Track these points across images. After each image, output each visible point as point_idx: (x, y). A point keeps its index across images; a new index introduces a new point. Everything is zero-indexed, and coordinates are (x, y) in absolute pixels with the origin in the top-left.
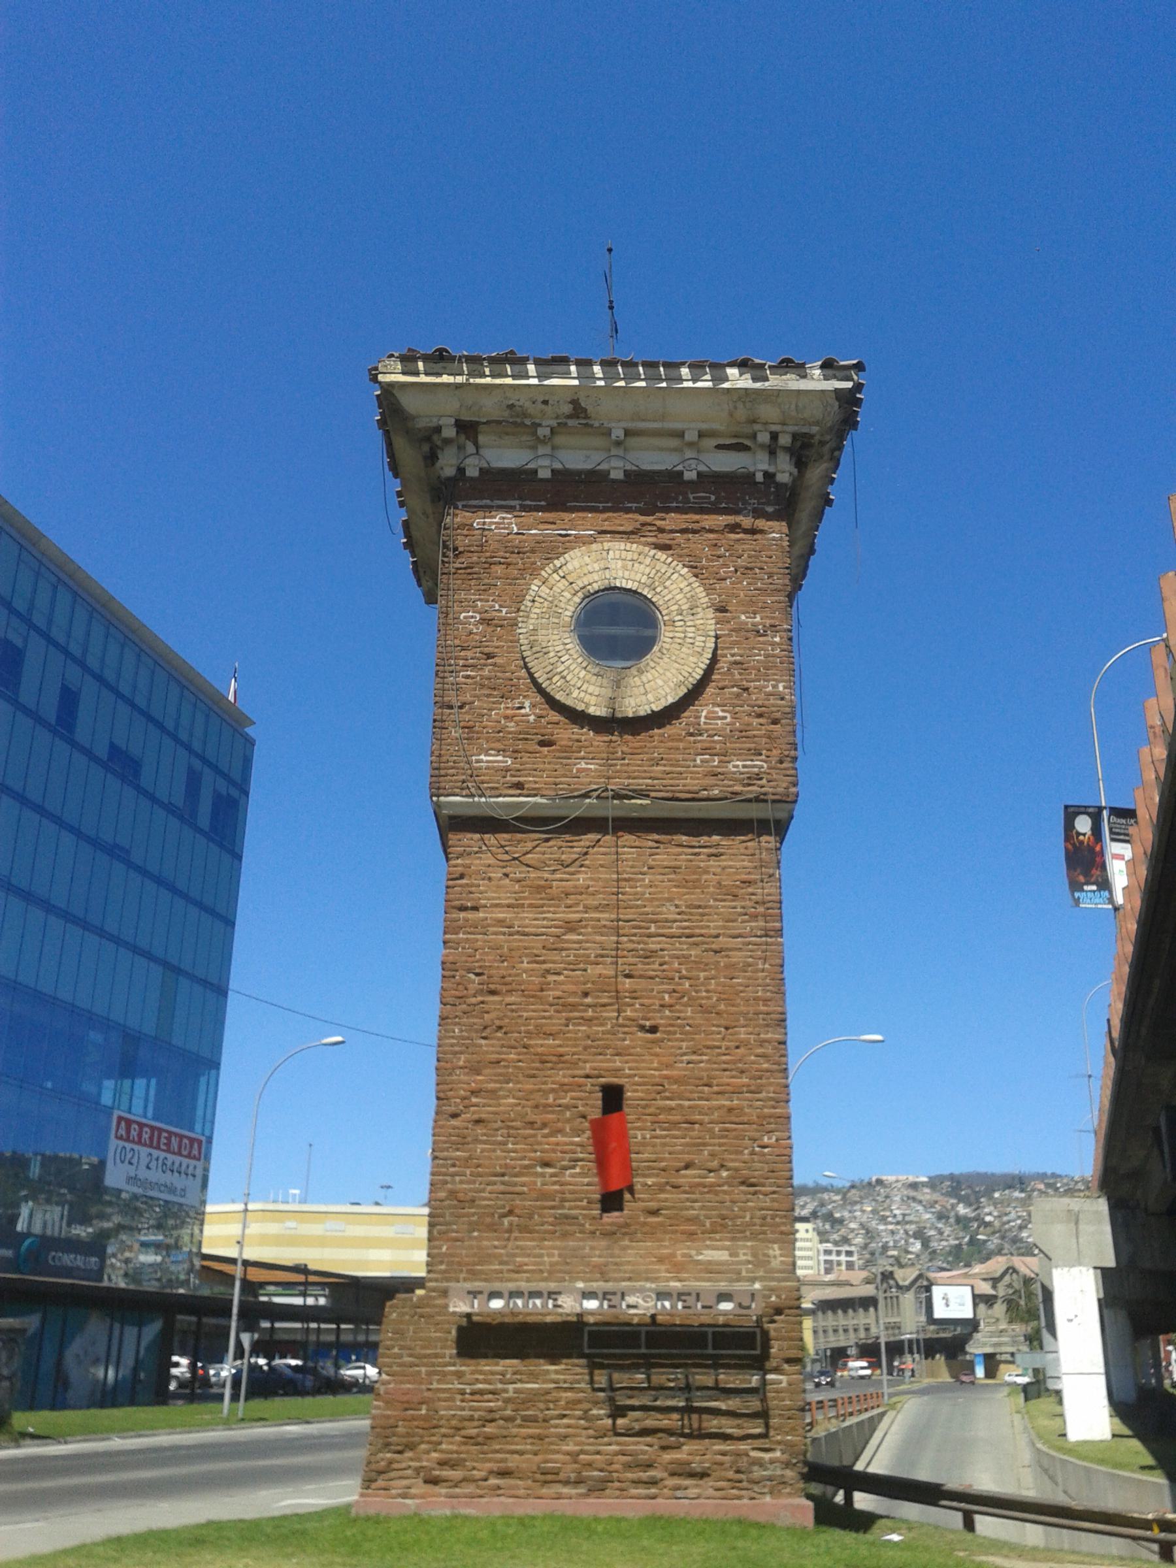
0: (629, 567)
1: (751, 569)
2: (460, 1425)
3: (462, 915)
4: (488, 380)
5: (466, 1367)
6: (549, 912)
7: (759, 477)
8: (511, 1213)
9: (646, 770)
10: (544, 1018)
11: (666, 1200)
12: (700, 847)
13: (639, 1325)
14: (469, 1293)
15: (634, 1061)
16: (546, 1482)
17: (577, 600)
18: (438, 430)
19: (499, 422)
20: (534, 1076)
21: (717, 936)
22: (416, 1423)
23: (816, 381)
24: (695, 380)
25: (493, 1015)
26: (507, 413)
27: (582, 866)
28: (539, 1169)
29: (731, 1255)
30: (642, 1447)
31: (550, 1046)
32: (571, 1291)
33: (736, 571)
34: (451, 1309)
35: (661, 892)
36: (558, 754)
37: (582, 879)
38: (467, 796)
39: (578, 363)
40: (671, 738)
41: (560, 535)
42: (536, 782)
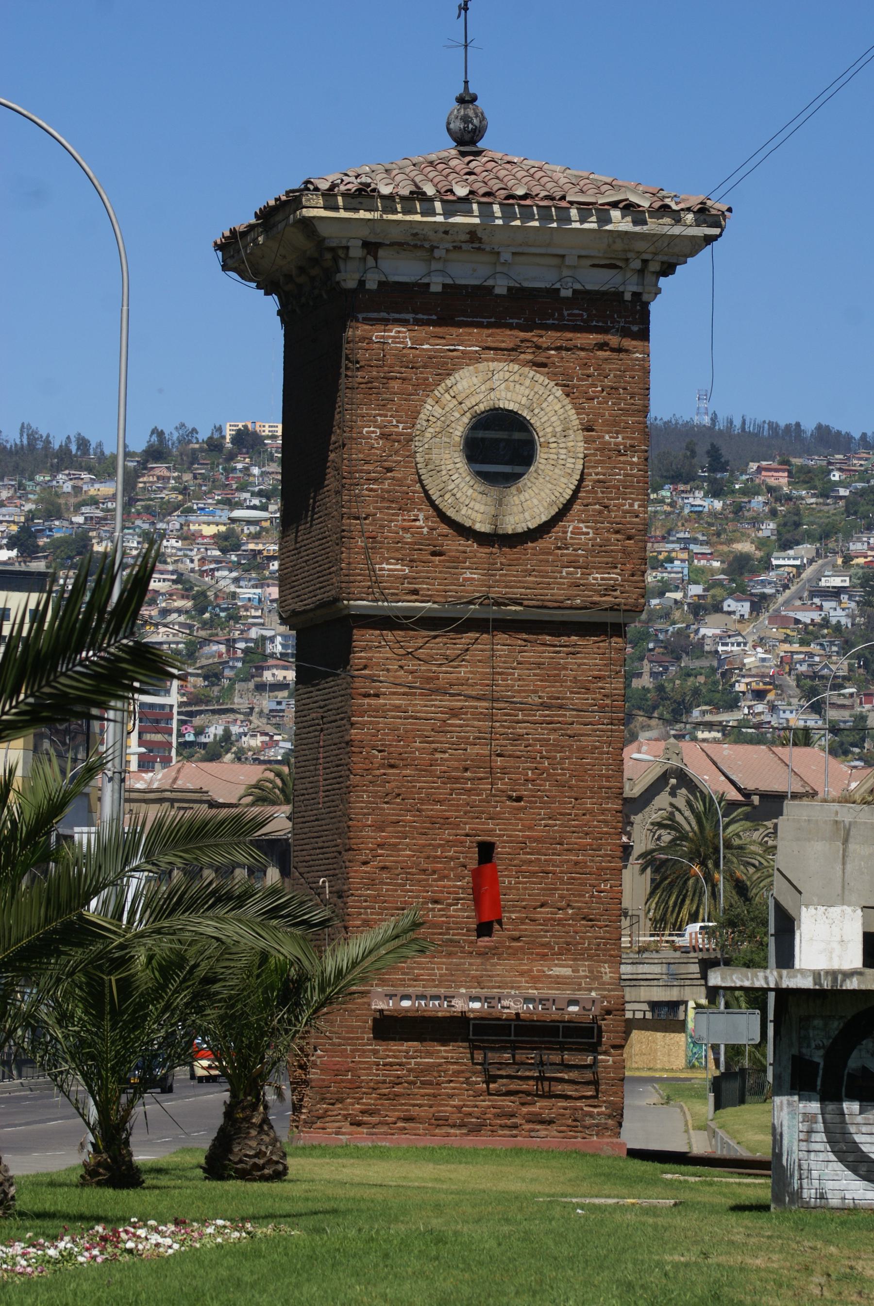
0: (511, 388)
1: (617, 389)
3: (366, 701)
7: (628, 297)
9: (522, 582)
10: (433, 788)
11: (526, 930)
12: (561, 646)
13: (506, 1020)
15: (504, 824)
17: (466, 420)
19: (400, 244)
24: (582, 221)
25: (394, 784)
27: (463, 660)
28: (430, 905)
30: (507, 1103)
31: (437, 810)
32: (461, 996)
33: (603, 390)
35: (527, 685)
42: (429, 590)
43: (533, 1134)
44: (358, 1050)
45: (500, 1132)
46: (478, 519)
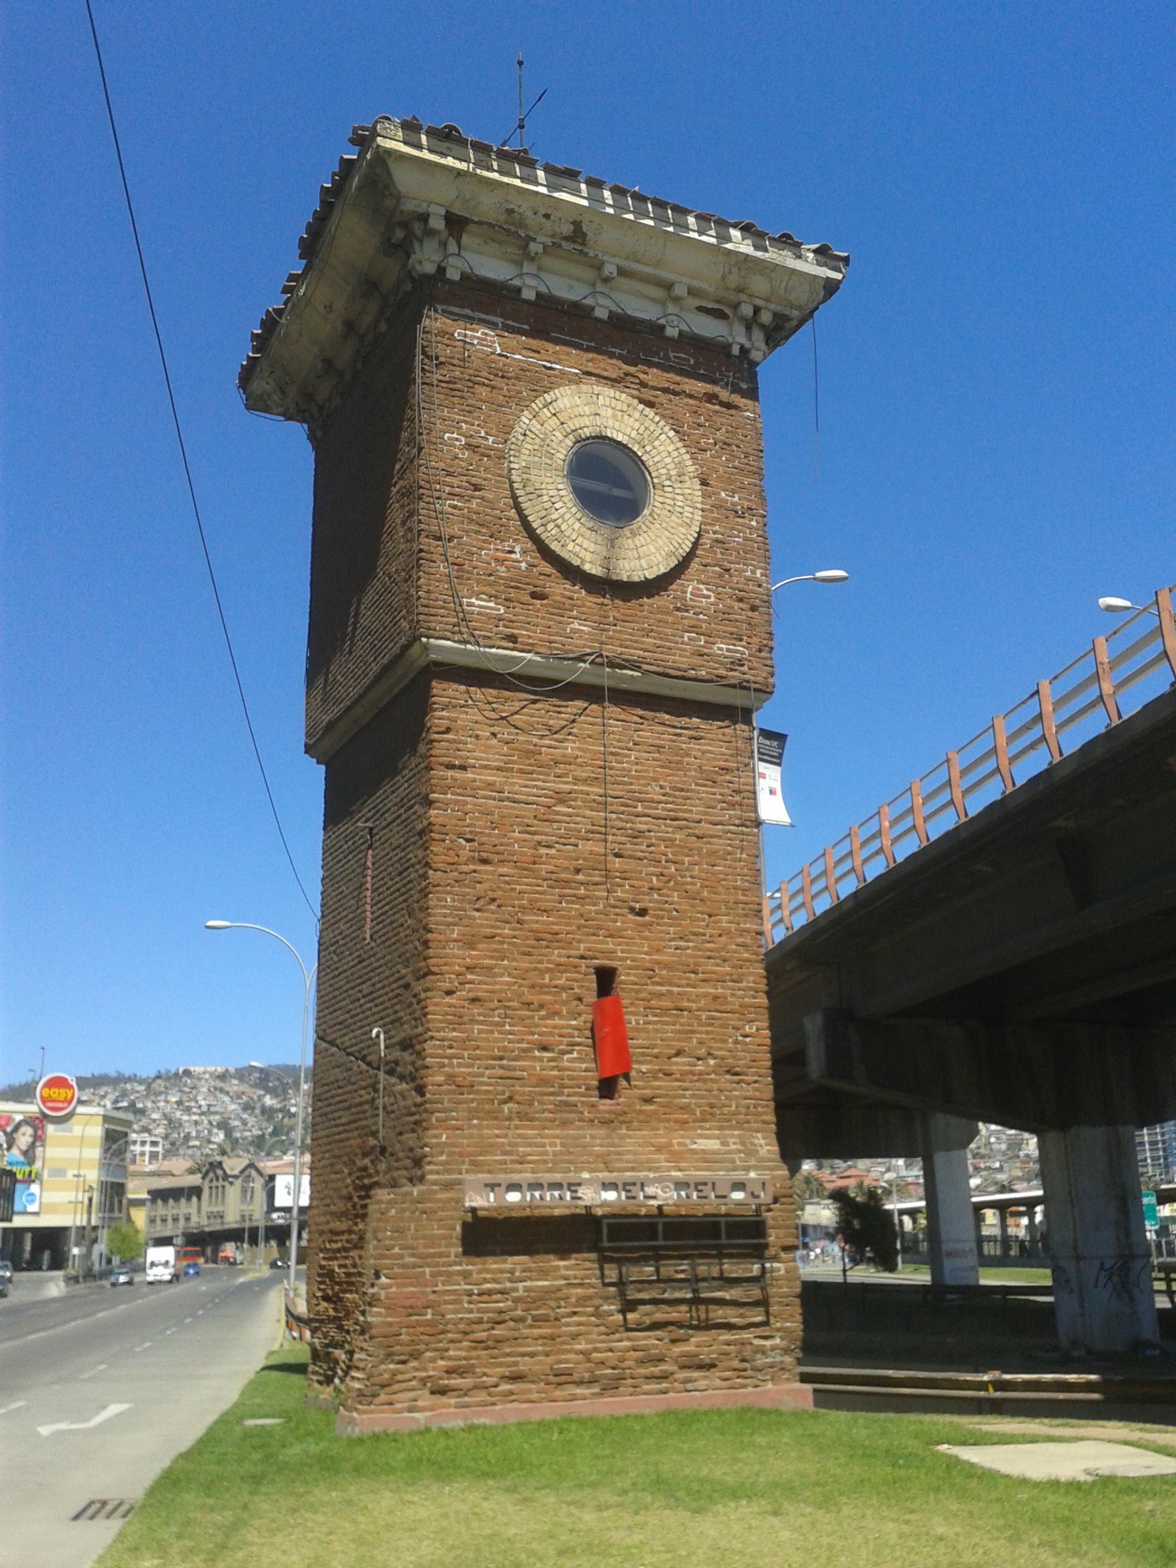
1: (729, 445)
2: (468, 1329)
3: (450, 773)
4: (495, 176)
5: (473, 1266)
6: (539, 780)
7: (736, 350)
8: (510, 1099)
10: (537, 892)
11: (660, 1088)
12: (682, 728)
14: (486, 1185)
15: (627, 944)
16: (560, 1384)
17: (569, 442)
18: (424, 218)
19: (492, 226)
20: (529, 954)
21: (699, 822)
22: (422, 1329)
23: (808, 265)
24: (701, 233)
25: (486, 886)
26: (503, 218)
27: (570, 734)
28: (537, 1053)
29: (722, 1144)
30: (650, 1340)
31: (543, 923)
32: (589, 1182)
34: (467, 1204)
35: (646, 771)
36: (551, 610)
37: (570, 748)
38: (459, 642)
39: (590, 182)
40: (660, 610)
41: (544, 366)
42: (530, 637)
43: (689, 1386)
44: (440, 1274)
45: (646, 1387)
46: (588, 559)
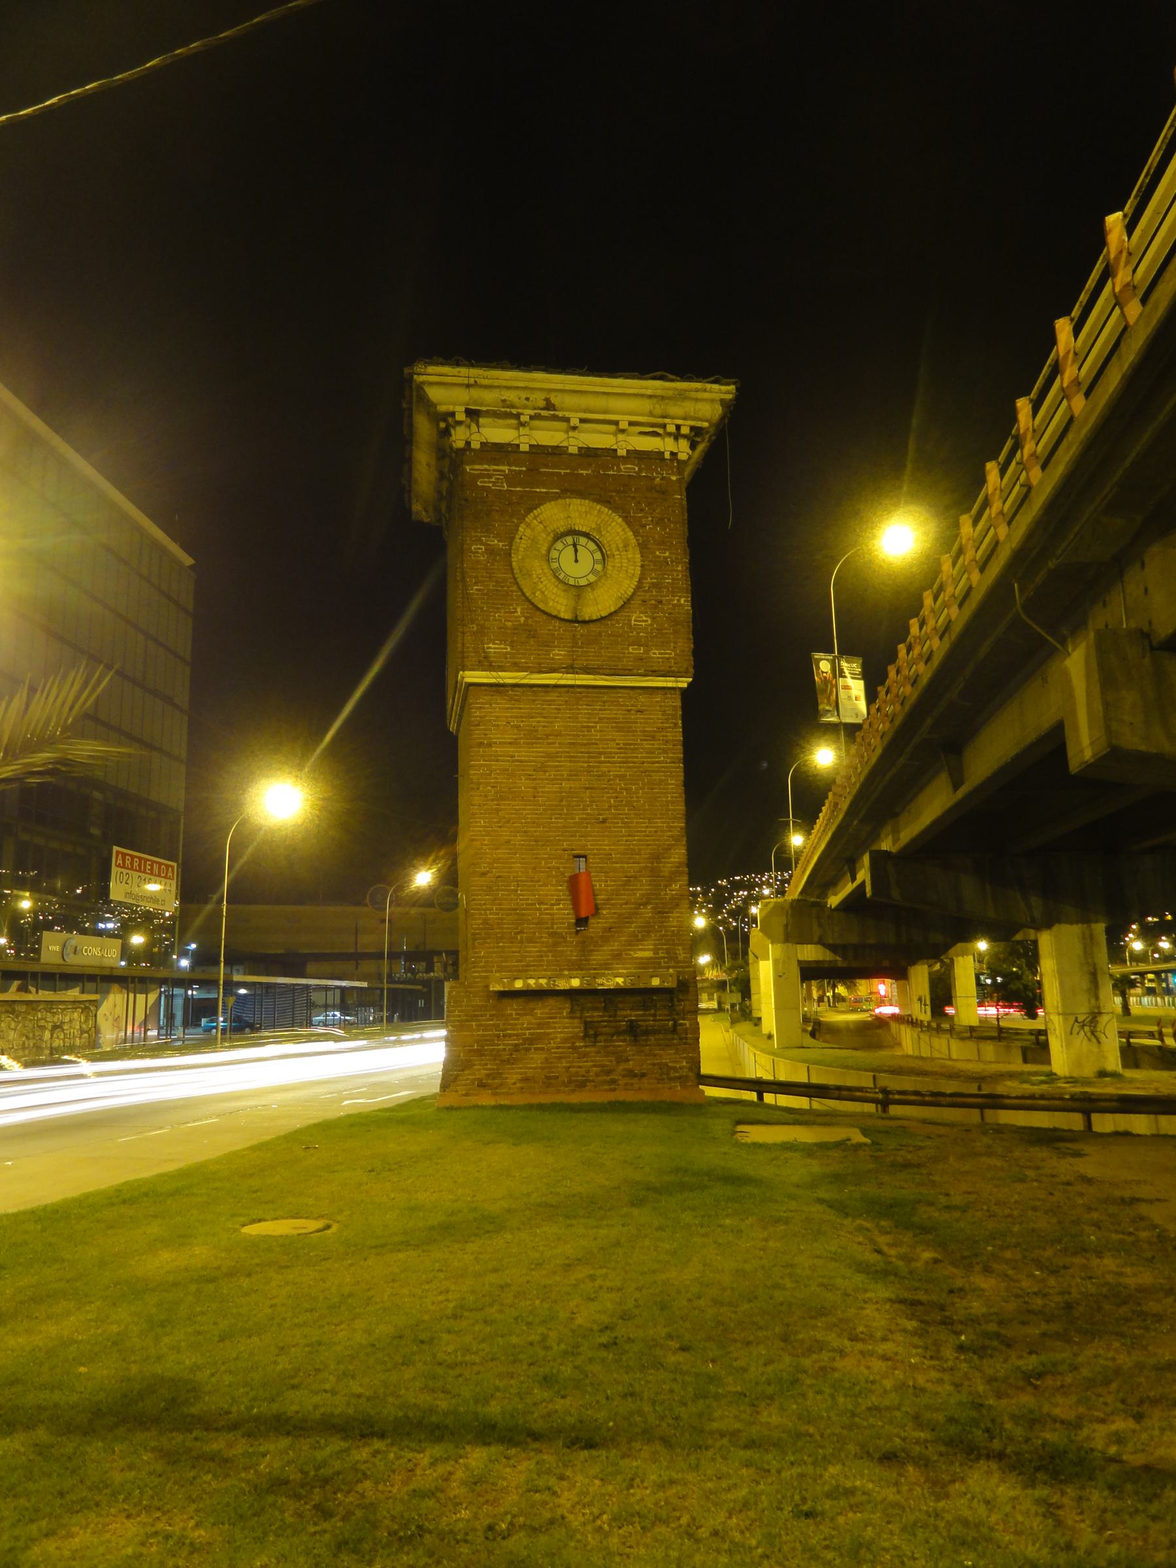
7: (667, 456)
18: (453, 414)
44: (481, 1025)
